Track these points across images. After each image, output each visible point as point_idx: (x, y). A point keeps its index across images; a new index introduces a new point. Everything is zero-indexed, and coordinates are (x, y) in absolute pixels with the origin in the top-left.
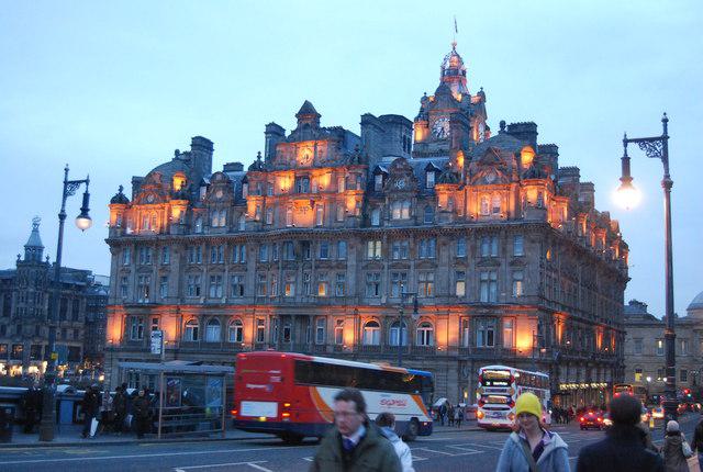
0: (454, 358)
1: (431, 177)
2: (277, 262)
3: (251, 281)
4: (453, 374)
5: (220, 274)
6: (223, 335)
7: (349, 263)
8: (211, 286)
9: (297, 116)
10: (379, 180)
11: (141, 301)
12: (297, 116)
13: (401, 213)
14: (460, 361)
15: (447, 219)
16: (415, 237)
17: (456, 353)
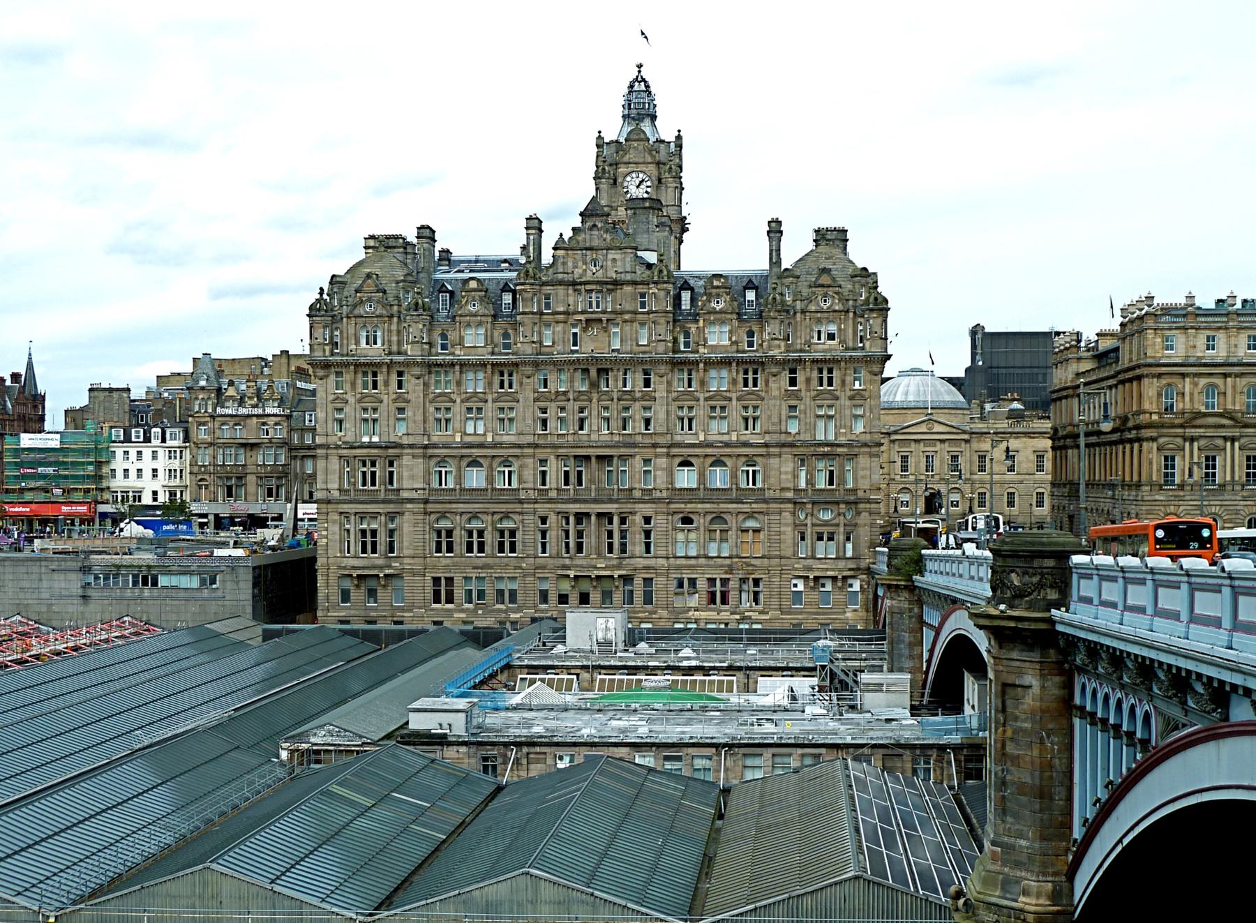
0: (789, 501)
1: (750, 295)
2: (565, 393)
3: (529, 414)
4: (787, 517)
5: (480, 405)
6: (490, 479)
7: (657, 395)
8: (468, 419)
9: (581, 214)
10: (686, 296)
11: (366, 439)
12: (581, 214)
13: (718, 337)
14: (795, 503)
15: (779, 347)
16: (738, 364)
17: (790, 495)
